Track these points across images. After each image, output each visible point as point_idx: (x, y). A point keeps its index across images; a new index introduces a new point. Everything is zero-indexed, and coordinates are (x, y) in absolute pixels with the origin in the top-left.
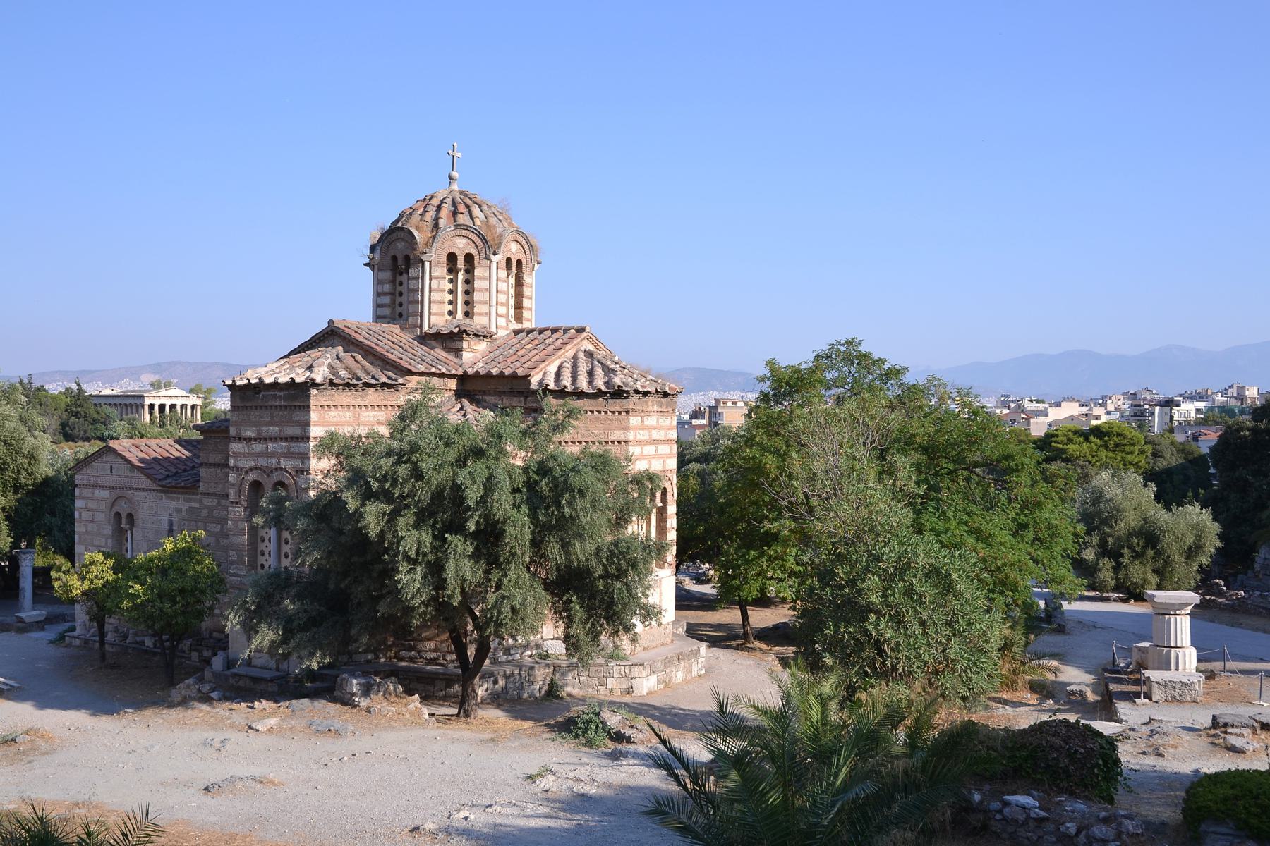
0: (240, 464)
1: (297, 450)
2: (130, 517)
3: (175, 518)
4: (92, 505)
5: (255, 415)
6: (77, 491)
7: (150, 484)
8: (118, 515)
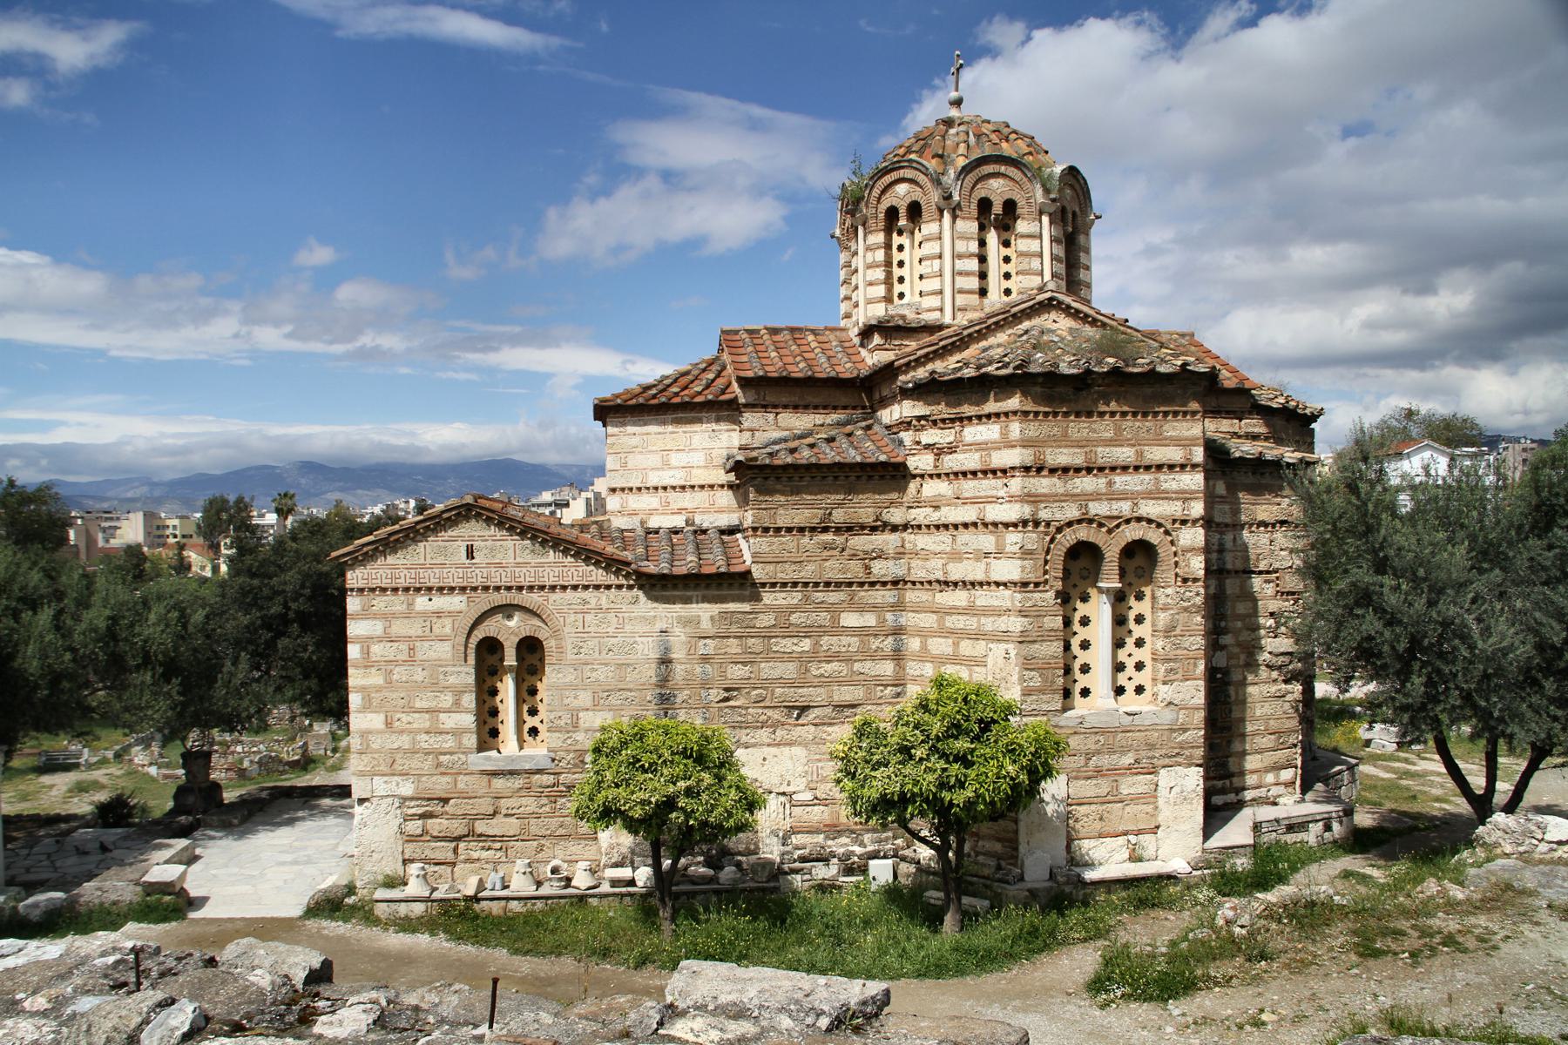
0: (1044, 515)
1: (1174, 486)
2: (531, 648)
3: (679, 638)
4: (398, 628)
5: (1078, 428)
6: (353, 604)
7: (598, 575)
8: (490, 649)
